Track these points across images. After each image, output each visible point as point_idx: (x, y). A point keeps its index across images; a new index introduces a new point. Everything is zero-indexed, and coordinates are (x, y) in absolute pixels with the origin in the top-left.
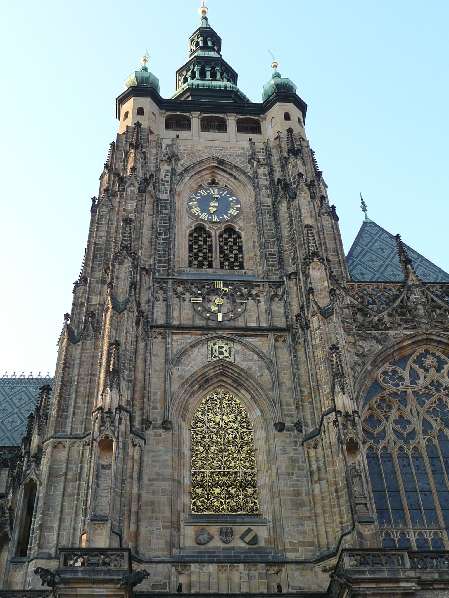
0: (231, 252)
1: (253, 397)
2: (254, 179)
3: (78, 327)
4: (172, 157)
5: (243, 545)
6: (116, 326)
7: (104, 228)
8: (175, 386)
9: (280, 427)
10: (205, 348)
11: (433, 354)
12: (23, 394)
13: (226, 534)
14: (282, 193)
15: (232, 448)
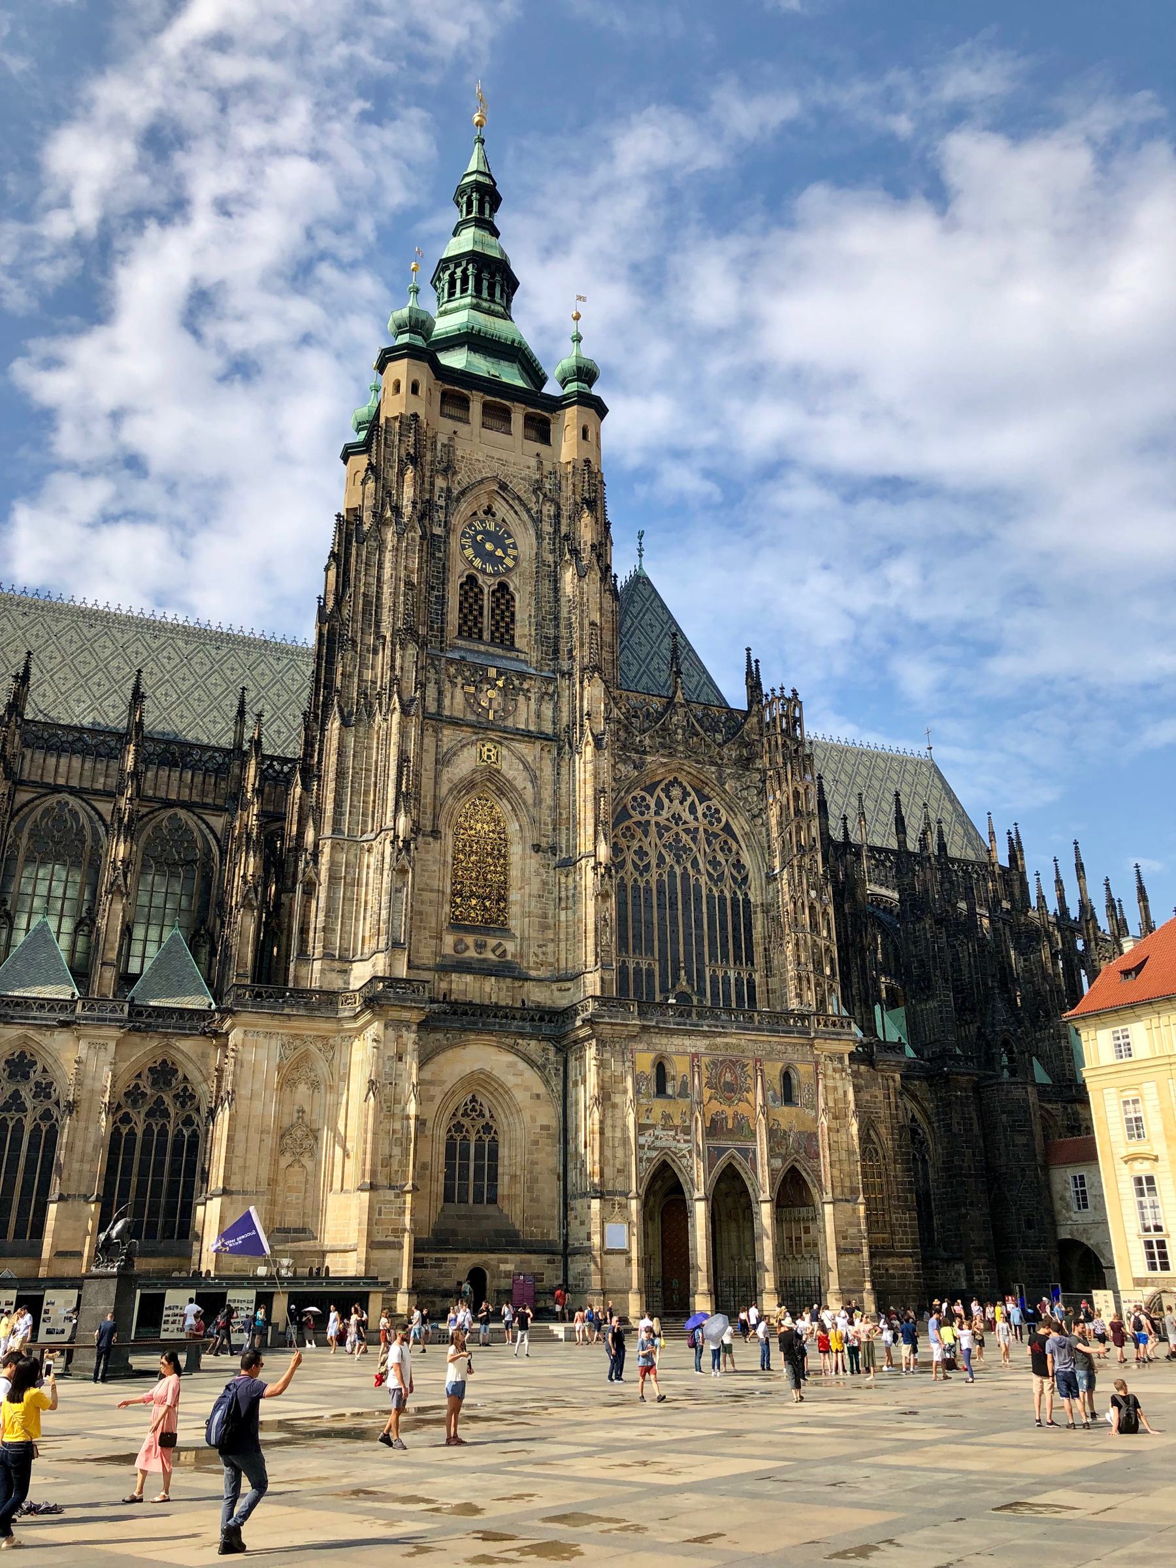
0: (502, 619)
1: (513, 809)
2: (537, 520)
3: (346, 706)
4: (448, 470)
5: (491, 956)
6: (403, 733)
7: (374, 571)
8: (444, 789)
9: (537, 848)
10: (474, 748)
11: (680, 784)
12: (170, 649)
13: (481, 947)
14: (568, 556)
15: (490, 860)
